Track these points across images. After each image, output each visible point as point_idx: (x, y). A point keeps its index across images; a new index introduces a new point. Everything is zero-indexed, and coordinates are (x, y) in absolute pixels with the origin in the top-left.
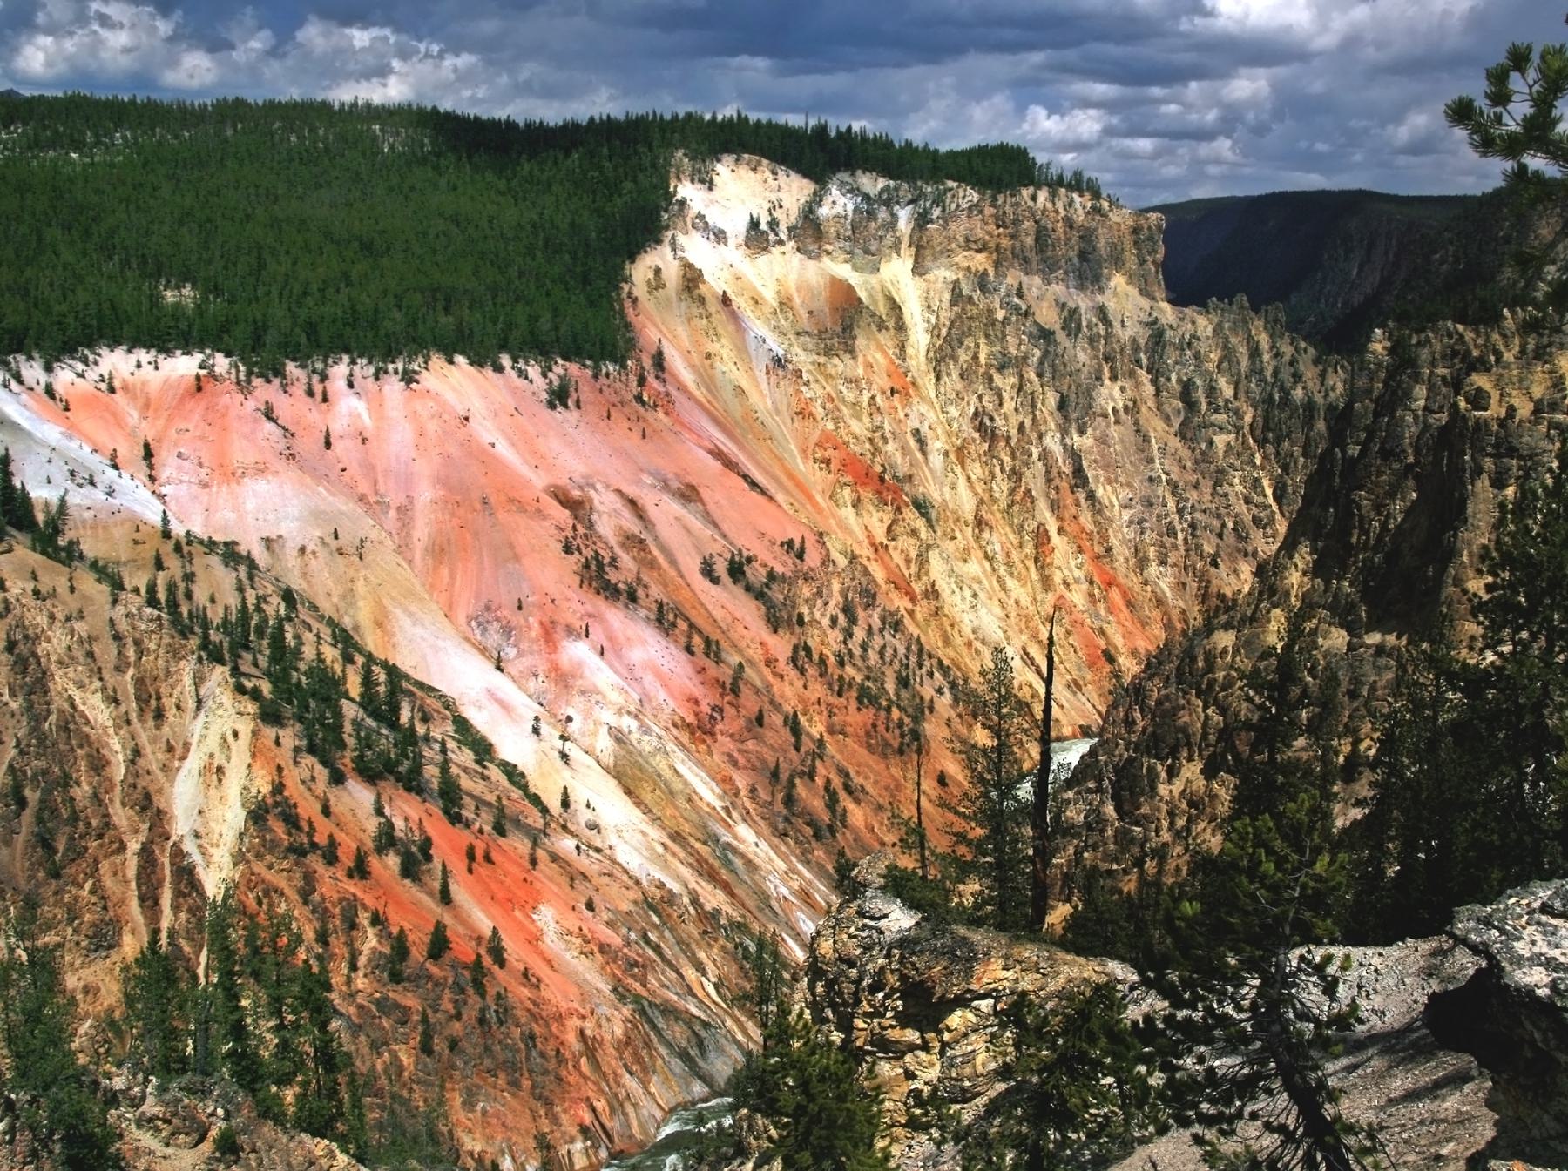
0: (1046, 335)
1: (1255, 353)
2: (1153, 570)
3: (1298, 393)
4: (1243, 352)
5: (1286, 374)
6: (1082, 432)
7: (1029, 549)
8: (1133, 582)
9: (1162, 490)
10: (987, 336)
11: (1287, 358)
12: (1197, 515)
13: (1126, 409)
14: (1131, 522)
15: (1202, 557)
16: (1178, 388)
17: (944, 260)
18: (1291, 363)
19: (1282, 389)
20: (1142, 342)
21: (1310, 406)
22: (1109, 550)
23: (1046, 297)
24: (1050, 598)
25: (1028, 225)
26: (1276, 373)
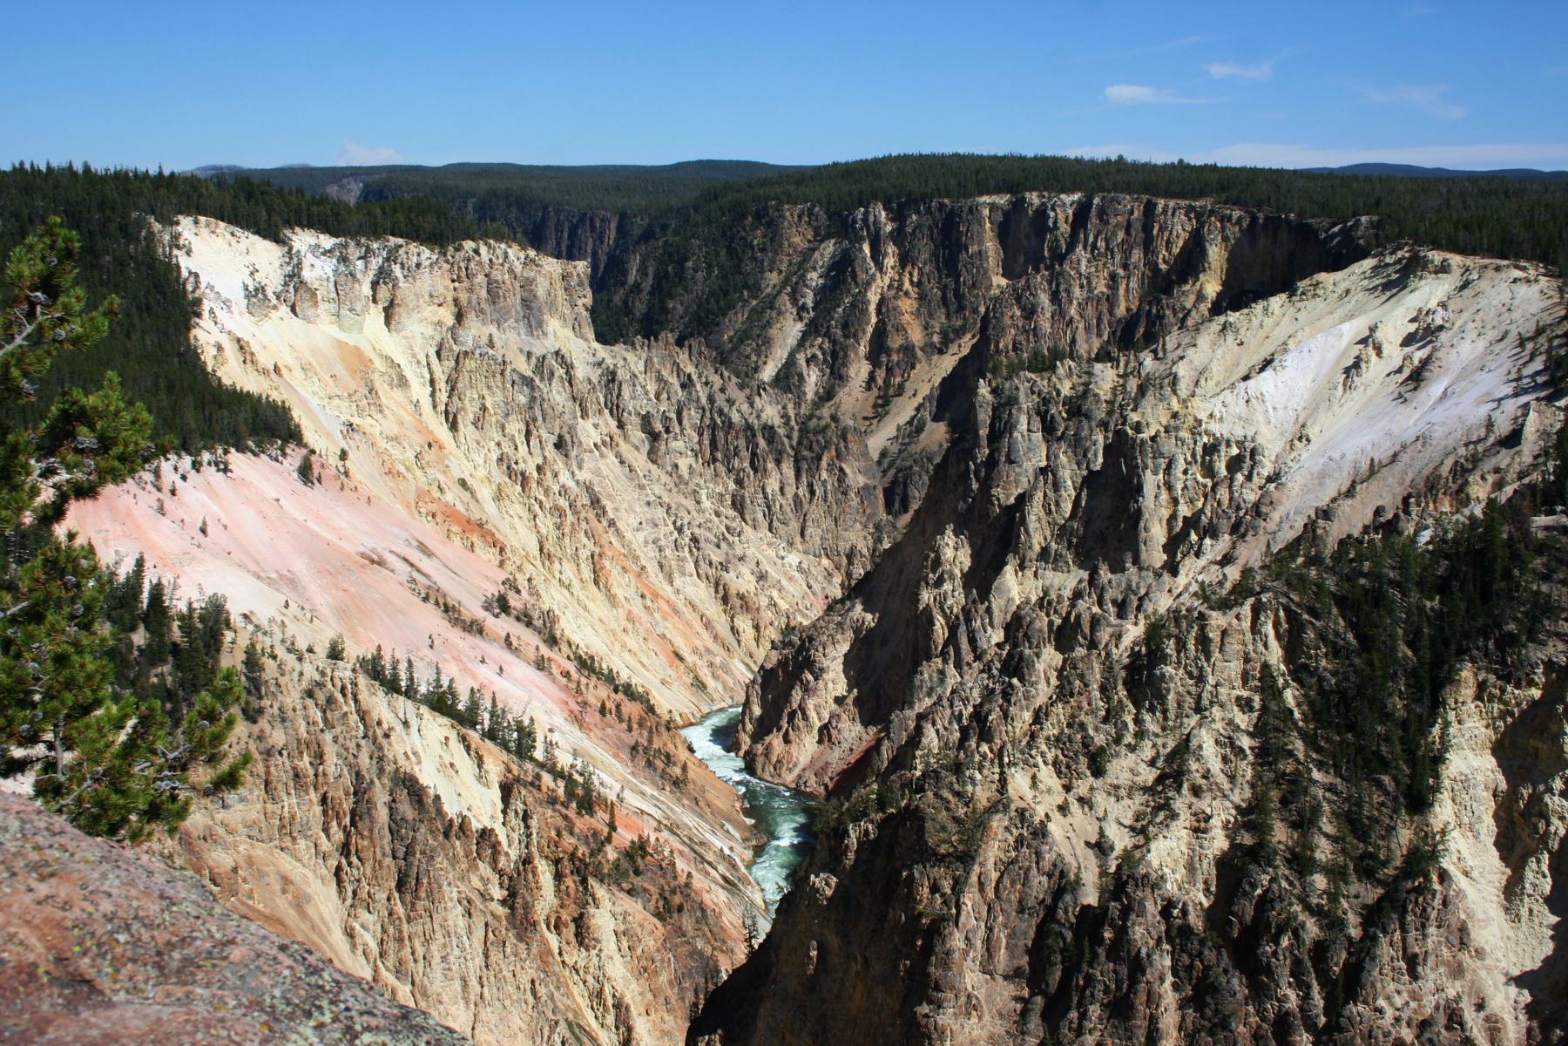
0: (528, 382)
1: (687, 384)
2: (678, 581)
3: (735, 417)
4: (674, 381)
5: (720, 400)
6: (580, 468)
7: (587, 573)
8: (667, 590)
9: (660, 513)
10: (489, 387)
11: (717, 386)
12: (697, 531)
13: (604, 443)
14: (646, 542)
15: (711, 564)
16: (638, 421)
17: (415, 316)
18: (722, 390)
19: (721, 412)
20: (595, 381)
21: (749, 427)
22: (643, 568)
23: (512, 342)
24: (622, 614)
25: (480, 279)
26: (711, 399)
